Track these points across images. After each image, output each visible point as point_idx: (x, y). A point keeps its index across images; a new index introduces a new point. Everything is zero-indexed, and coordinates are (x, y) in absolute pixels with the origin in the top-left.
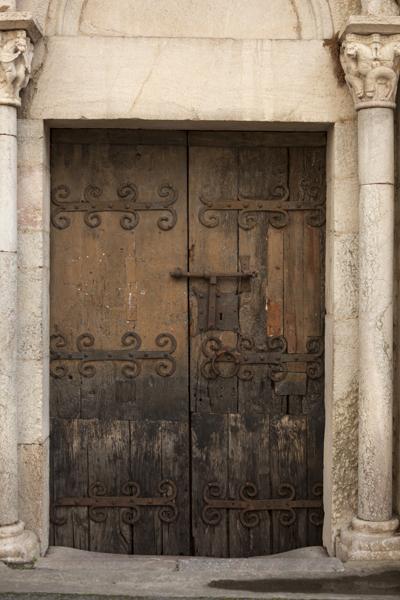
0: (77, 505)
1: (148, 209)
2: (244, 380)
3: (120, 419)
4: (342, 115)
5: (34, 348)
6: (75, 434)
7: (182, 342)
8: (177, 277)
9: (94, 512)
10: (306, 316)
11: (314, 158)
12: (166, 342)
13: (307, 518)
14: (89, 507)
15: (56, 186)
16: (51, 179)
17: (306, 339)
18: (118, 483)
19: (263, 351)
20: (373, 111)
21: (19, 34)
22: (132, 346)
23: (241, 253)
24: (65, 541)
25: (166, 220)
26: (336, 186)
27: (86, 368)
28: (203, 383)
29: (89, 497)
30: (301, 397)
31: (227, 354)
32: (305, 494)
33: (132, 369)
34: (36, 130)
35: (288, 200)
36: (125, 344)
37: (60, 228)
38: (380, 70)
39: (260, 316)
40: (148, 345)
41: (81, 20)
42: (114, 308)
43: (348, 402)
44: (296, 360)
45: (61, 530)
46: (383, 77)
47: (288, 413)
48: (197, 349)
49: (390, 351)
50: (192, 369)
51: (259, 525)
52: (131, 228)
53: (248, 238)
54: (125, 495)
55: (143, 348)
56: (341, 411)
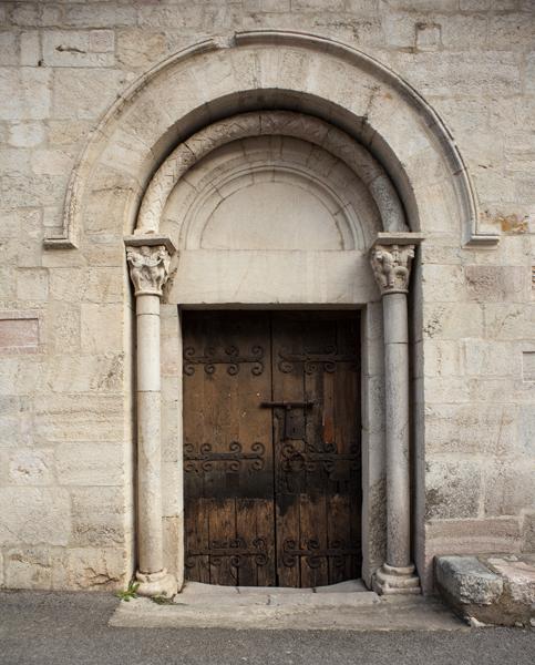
1: (245, 361)
6: (200, 508)
7: (269, 447)
8: (264, 406)
17: (349, 445)
20: (394, 296)
21: (161, 248)
23: (307, 389)
31: (299, 455)
33: (236, 465)
34: (174, 311)
36: (231, 449)
38: (398, 268)
39: (319, 430)
40: (246, 450)
41: (201, 239)
43: (378, 487)
45: (191, 571)
46: (400, 274)
47: (338, 492)
49: (407, 453)
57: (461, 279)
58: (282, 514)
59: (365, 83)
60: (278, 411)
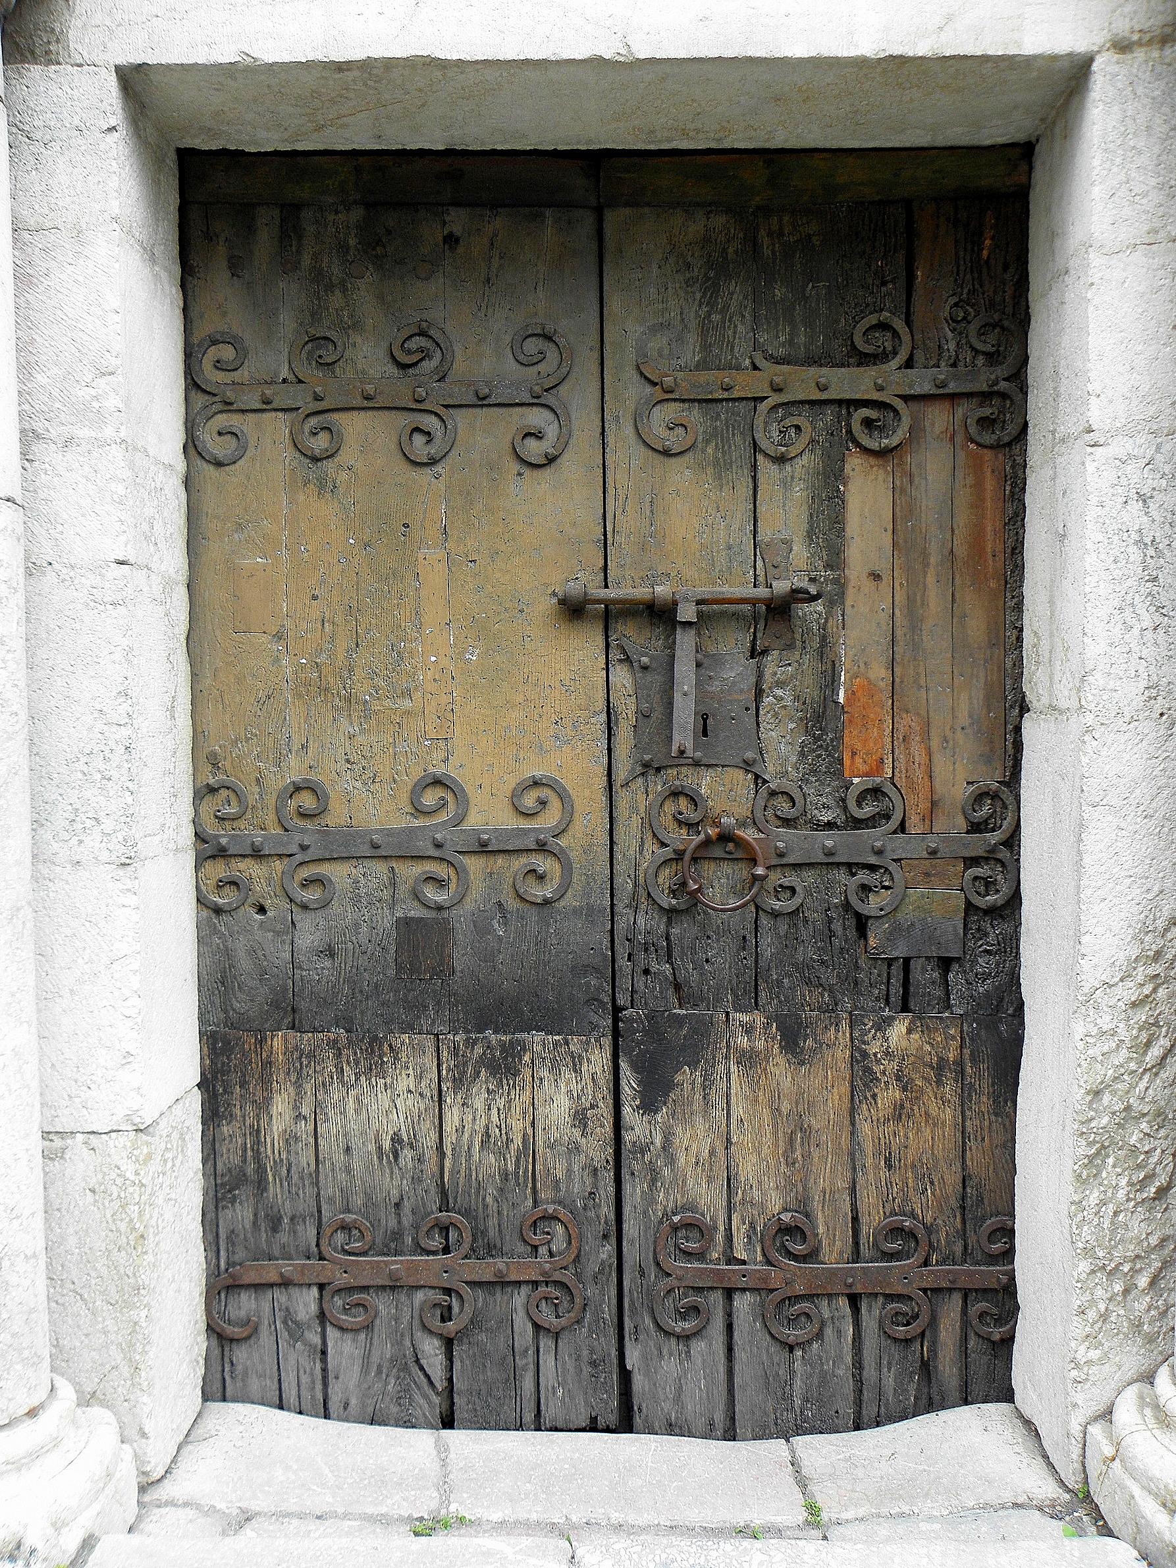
0: (286, 1283)
1: (482, 402)
2: (775, 915)
3: (408, 1028)
4: (1123, 26)
5: (108, 825)
9: (338, 1302)
10: (963, 718)
11: (988, 233)
12: (543, 803)
13: (964, 1311)
14: (321, 1287)
15: (202, 331)
16: (185, 310)
18: (407, 1221)
19: (830, 825)
22: (442, 817)
23: (765, 534)
24: (255, 1385)
25: (538, 436)
26: (1095, 275)
27: (306, 883)
28: (646, 922)
29: (322, 1258)
30: (945, 964)
31: (725, 838)
32: (958, 1249)
33: (440, 883)
35: (909, 364)
37: (219, 464)
42: (387, 703)
43: (1128, 992)
44: (933, 853)
45: (241, 1354)
47: (905, 1009)
48: (636, 821)
50: (618, 880)
51: (819, 1335)
52: (433, 462)
53: (786, 484)
54: (429, 1253)
55: (474, 821)
56: (1106, 1022)
58: (648, 1106)
60: (630, 633)
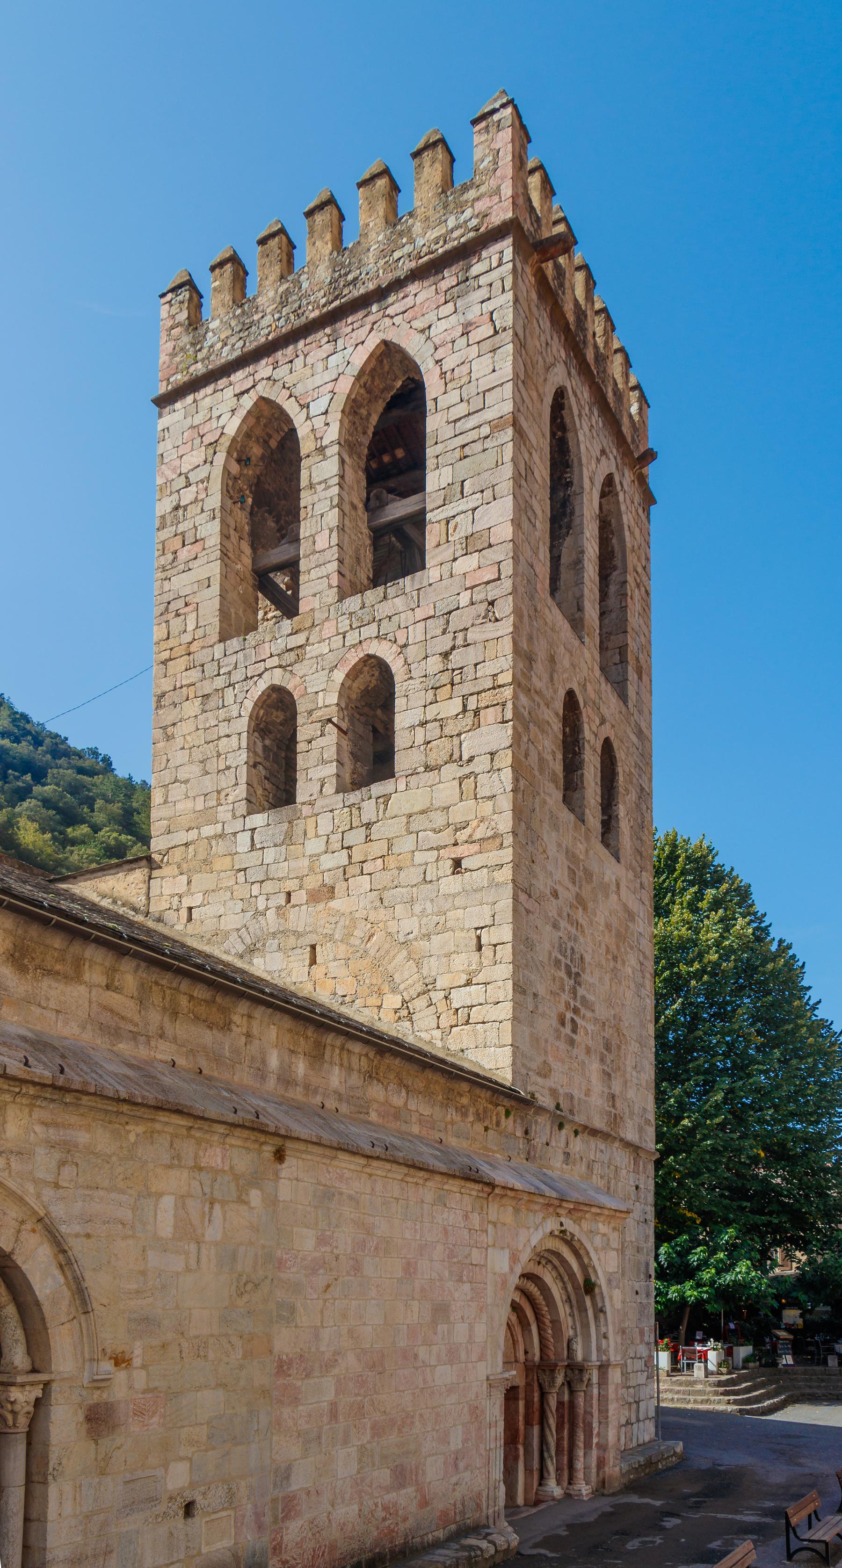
57: (81, 1417)
59: (14, 1215)
